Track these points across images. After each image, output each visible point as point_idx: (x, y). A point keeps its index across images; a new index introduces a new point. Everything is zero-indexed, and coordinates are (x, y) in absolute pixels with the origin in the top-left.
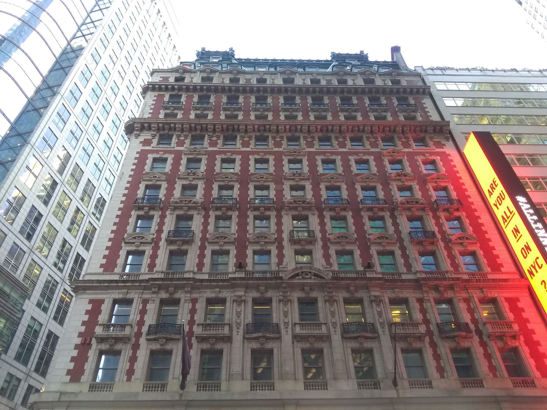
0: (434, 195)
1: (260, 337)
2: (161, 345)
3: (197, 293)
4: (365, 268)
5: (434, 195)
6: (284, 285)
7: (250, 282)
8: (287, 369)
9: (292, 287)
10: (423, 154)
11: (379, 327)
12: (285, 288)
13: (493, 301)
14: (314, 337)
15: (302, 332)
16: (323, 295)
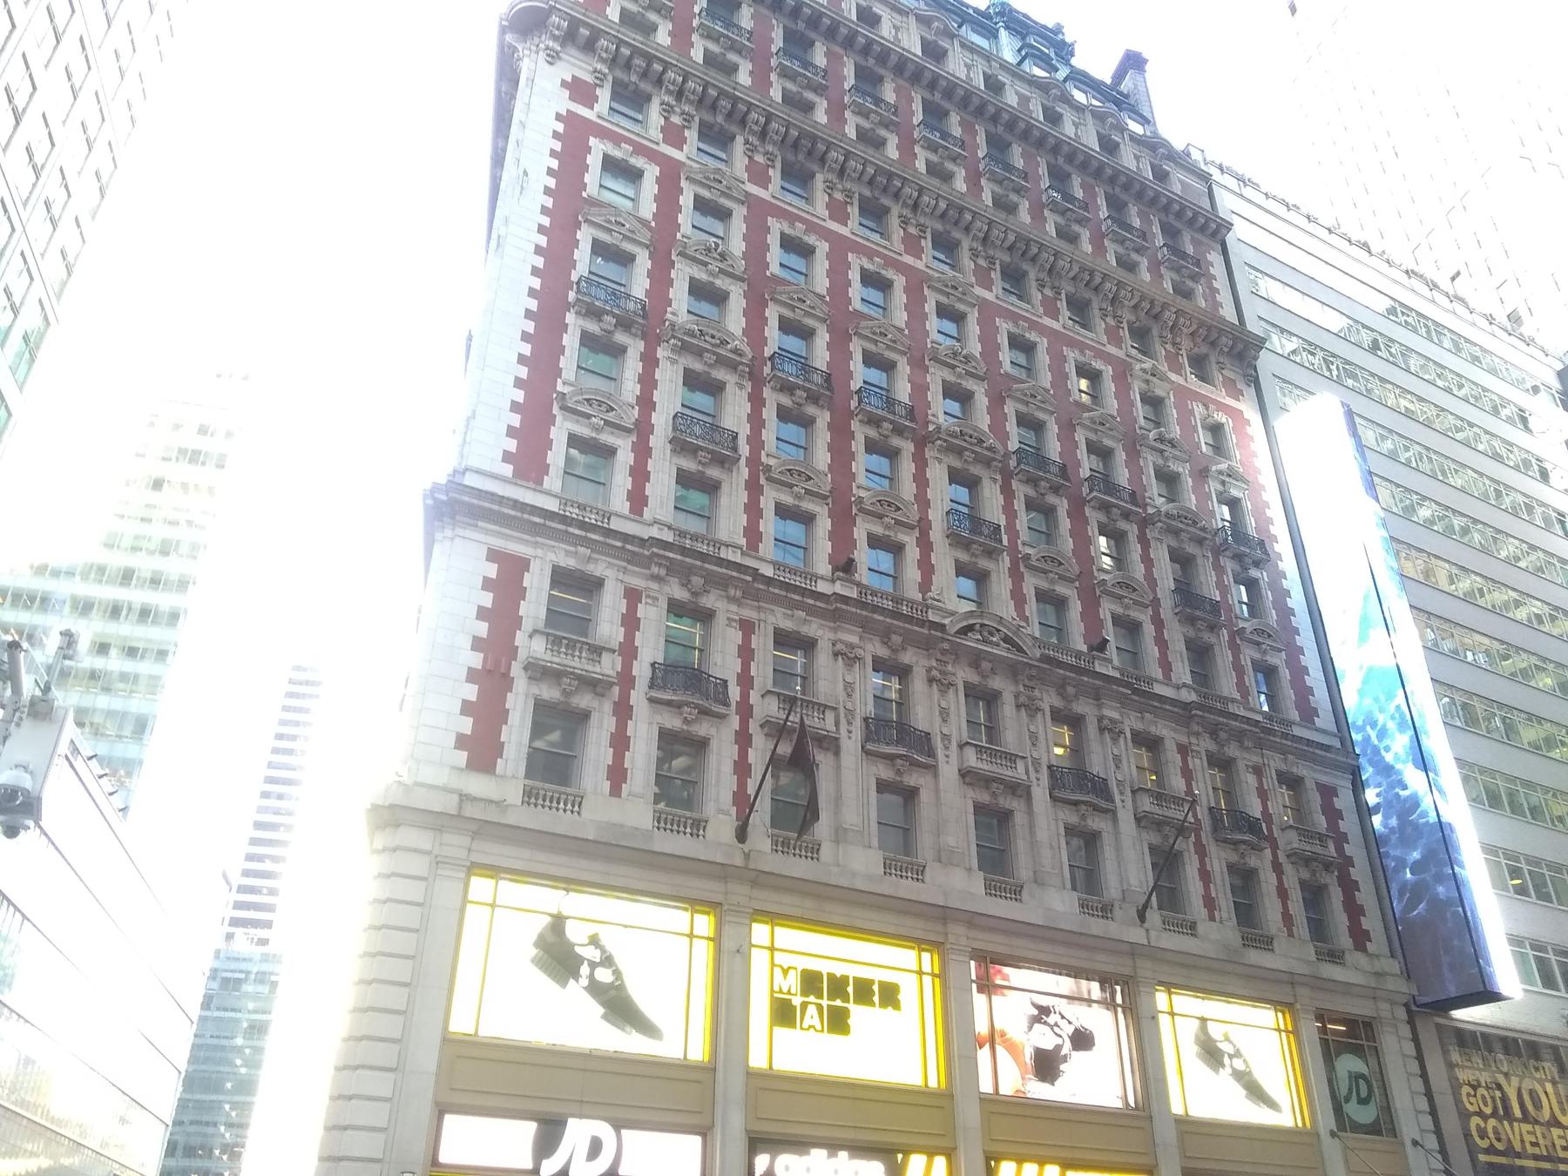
0: (860, 373)
1: (900, 756)
2: (686, 721)
3: (752, 607)
4: (1091, 648)
5: (860, 373)
6: (946, 646)
7: (876, 616)
8: (951, 841)
9: (956, 652)
10: (1014, 317)
11: (1115, 790)
12: (944, 652)
13: (1293, 783)
14: (1001, 781)
15: (980, 765)
16: (926, 663)
